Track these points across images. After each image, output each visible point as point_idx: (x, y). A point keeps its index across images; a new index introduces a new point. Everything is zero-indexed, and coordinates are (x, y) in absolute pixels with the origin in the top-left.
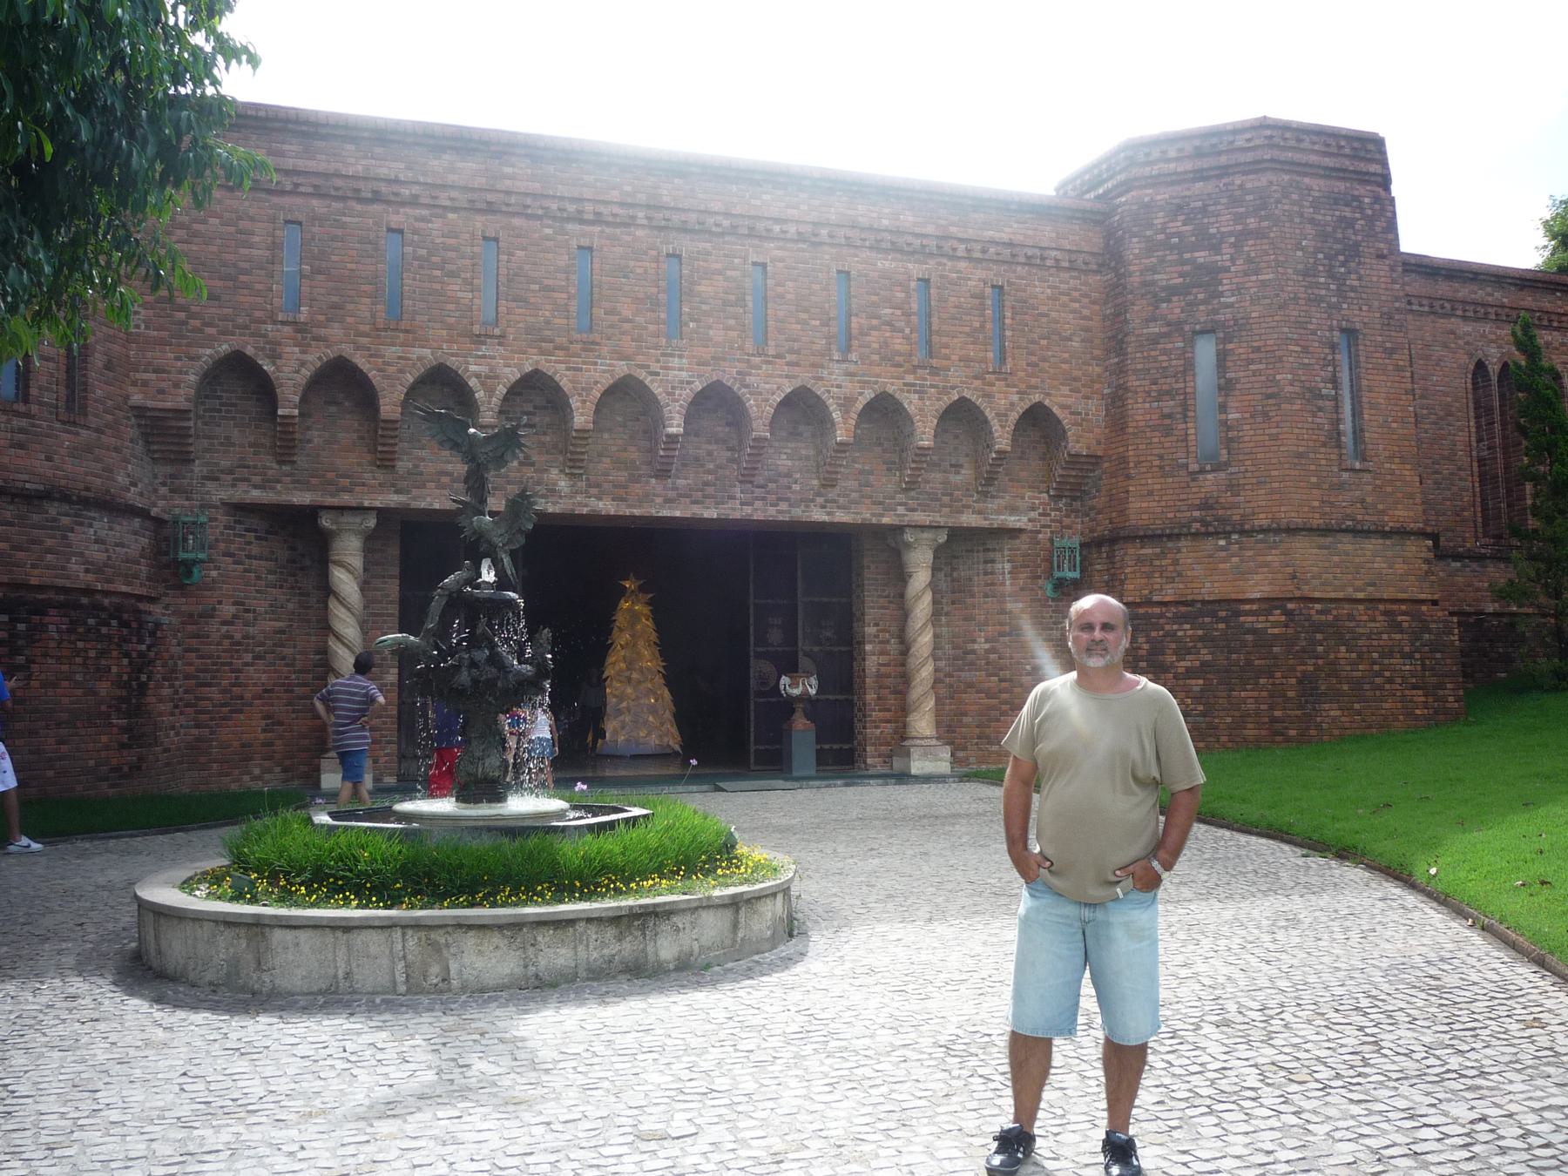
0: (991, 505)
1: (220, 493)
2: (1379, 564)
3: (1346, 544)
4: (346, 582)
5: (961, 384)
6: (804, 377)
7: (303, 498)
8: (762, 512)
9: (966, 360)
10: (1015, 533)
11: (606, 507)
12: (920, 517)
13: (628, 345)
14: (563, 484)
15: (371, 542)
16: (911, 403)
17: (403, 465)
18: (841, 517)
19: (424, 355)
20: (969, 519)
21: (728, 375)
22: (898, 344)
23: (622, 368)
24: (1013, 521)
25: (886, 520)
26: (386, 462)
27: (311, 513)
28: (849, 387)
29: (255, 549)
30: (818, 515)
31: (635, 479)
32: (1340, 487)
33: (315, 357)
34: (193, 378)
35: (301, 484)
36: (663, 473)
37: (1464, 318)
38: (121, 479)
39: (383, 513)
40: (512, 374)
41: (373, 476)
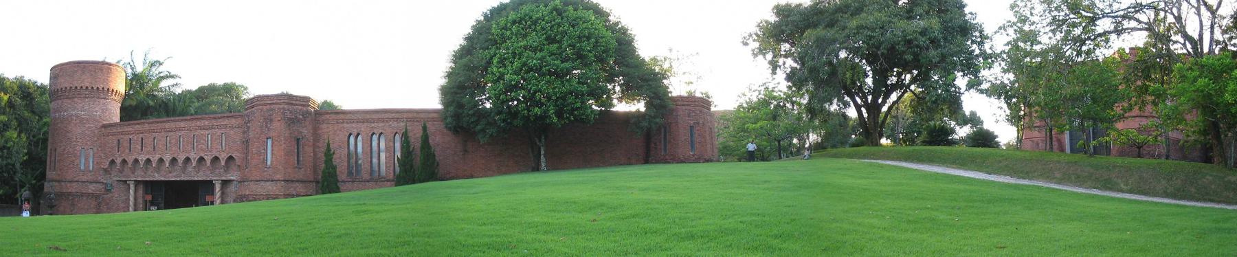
0: (228, 175)
1: (115, 179)
2: (270, 187)
3: (262, 183)
4: (132, 192)
5: (215, 153)
6: (187, 155)
7: (124, 179)
8: (186, 179)
9: (216, 149)
10: (234, 180)
11: (163, 179)
12: (214, 178)
13: (161, 153)
14: (157, 175)
15: (136, 186)
16: (206, 158)
17: (136, 174)
18: (200, 179)
19: (134, 157)
20: (224, 178)
21: (175, 156)
22: (204, 147)
23: (160, 156)
24: (232, 178)
25: (208, 179)
26: (133, 173)
27: (126, 181)
28: (195, 156)
29: (122, 186)
30: (196, 179)
31: (167, 174)
32: (264, 171)
33: (121, 159)
34: (108, 163)
35: (124, 176)
36: (170, 173)
37: (347, 123)
38: (100, 178)
39: (134, 181)
40: (145, 159)
41: (132, 175)
